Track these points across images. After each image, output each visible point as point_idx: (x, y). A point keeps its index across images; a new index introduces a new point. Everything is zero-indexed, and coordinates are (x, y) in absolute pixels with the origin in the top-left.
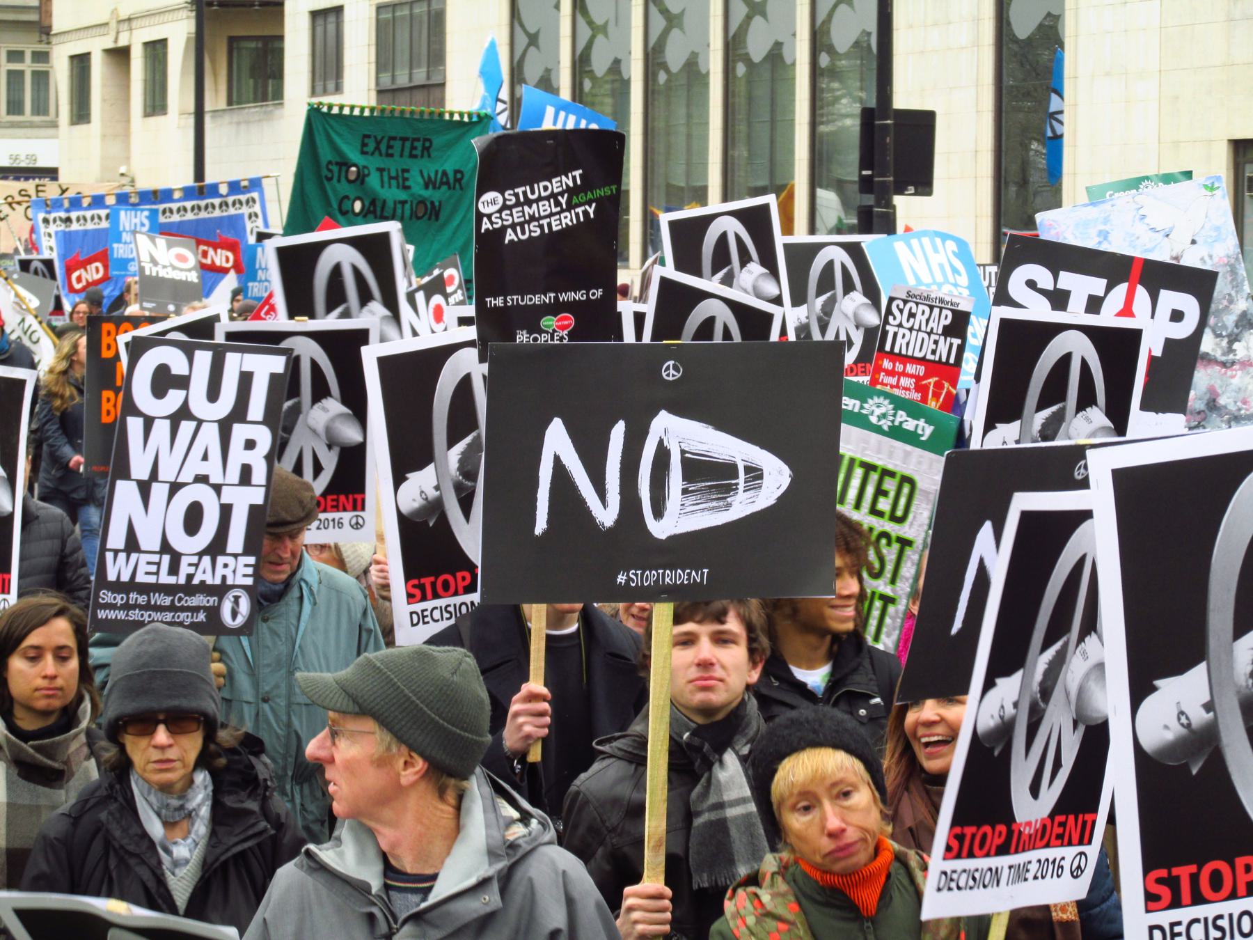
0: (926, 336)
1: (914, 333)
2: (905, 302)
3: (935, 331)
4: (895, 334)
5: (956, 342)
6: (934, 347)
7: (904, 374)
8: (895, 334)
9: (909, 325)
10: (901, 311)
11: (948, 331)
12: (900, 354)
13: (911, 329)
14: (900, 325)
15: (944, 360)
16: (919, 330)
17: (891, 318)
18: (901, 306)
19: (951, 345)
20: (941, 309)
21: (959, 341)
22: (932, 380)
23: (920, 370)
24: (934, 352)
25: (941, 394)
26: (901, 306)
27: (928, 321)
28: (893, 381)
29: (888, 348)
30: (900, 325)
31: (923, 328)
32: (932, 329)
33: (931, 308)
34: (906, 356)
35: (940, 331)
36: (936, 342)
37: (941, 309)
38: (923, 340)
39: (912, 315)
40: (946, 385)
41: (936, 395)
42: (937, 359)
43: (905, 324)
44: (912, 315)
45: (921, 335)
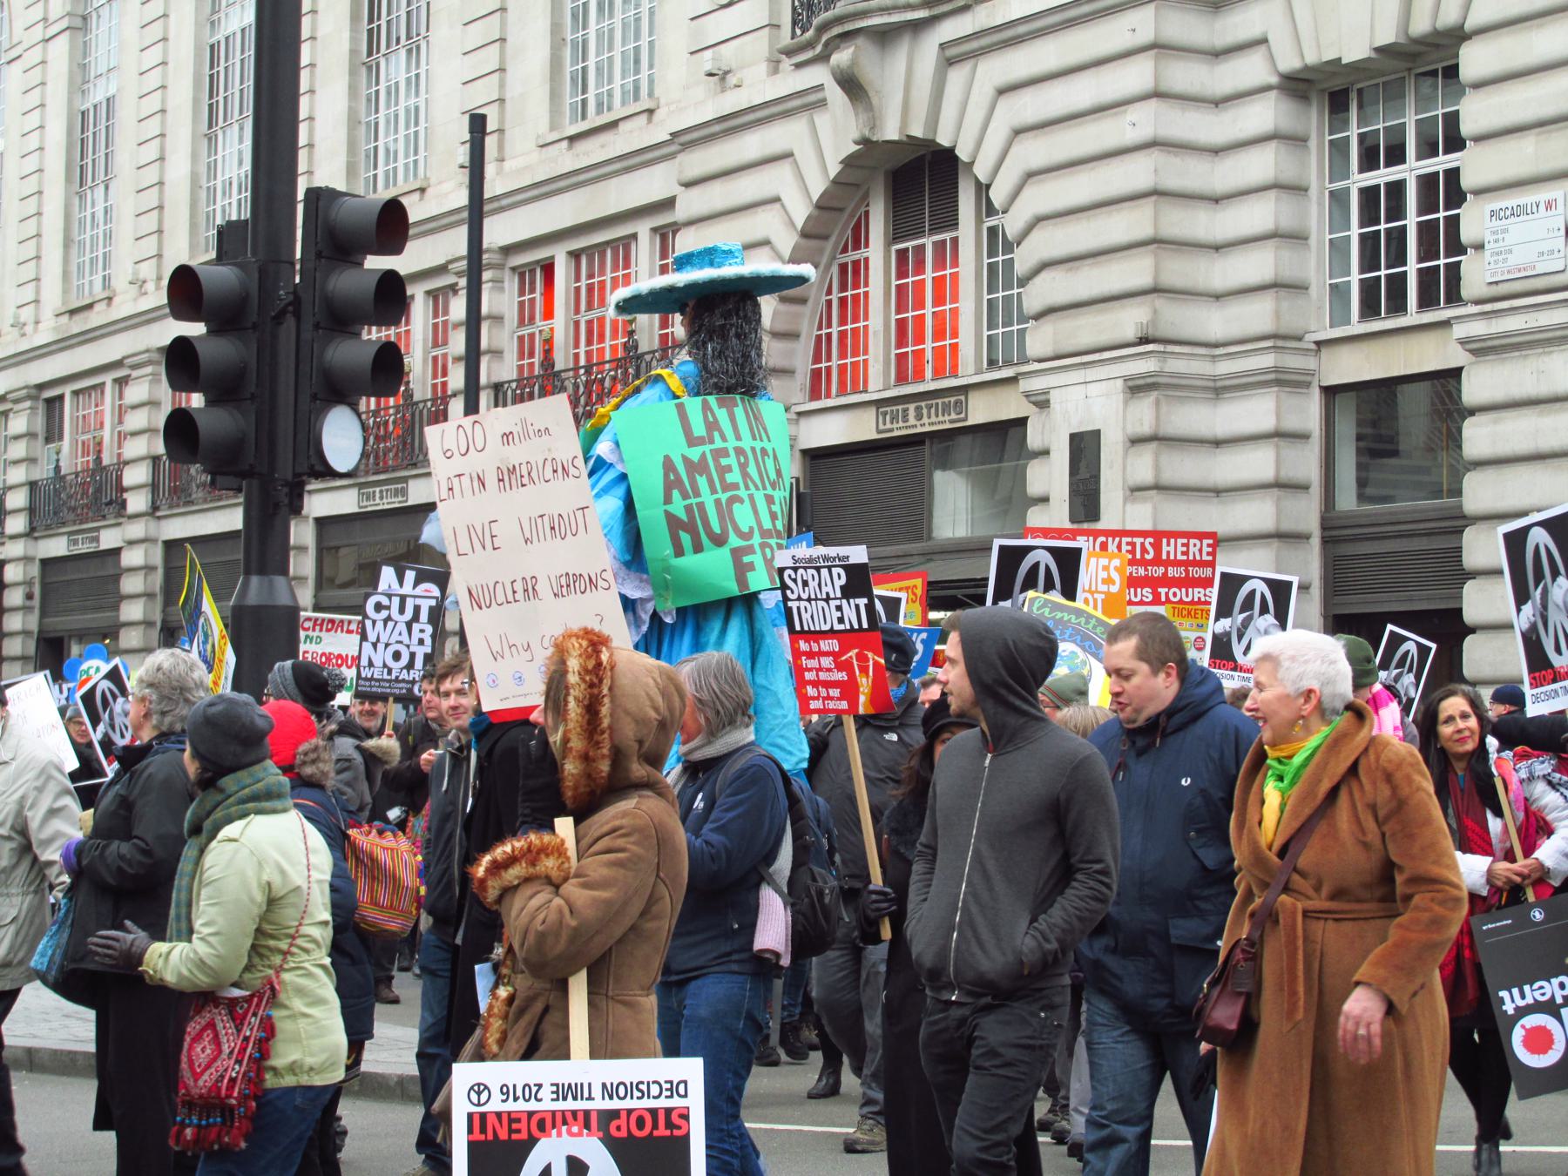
2: (795, 569)
3: (832, 596)
5: (862, 602)
6: (839, 614)
7: (821, 654)
8: (799, 608)
9: (805, 596)
11: (848, 592)
12: (810, 632)
13: (809, 600)
14: (799, 599)
15: (856, 626)
17: (788, 592)
18: (793, 576)
19: (857, 607)
20: (829, 568)
21: (865, 601)
22: (853, 653)
24: (841, 620)
29: (798, 628)
32: (827, 594)
33: (818, 569)
34: (815, 632)
35: (839, 594)
36: (839, 608)
39: (805, 583)
40: (870, 655)
41: (864, 670)
42: (848, 627)
44: (805, 583)
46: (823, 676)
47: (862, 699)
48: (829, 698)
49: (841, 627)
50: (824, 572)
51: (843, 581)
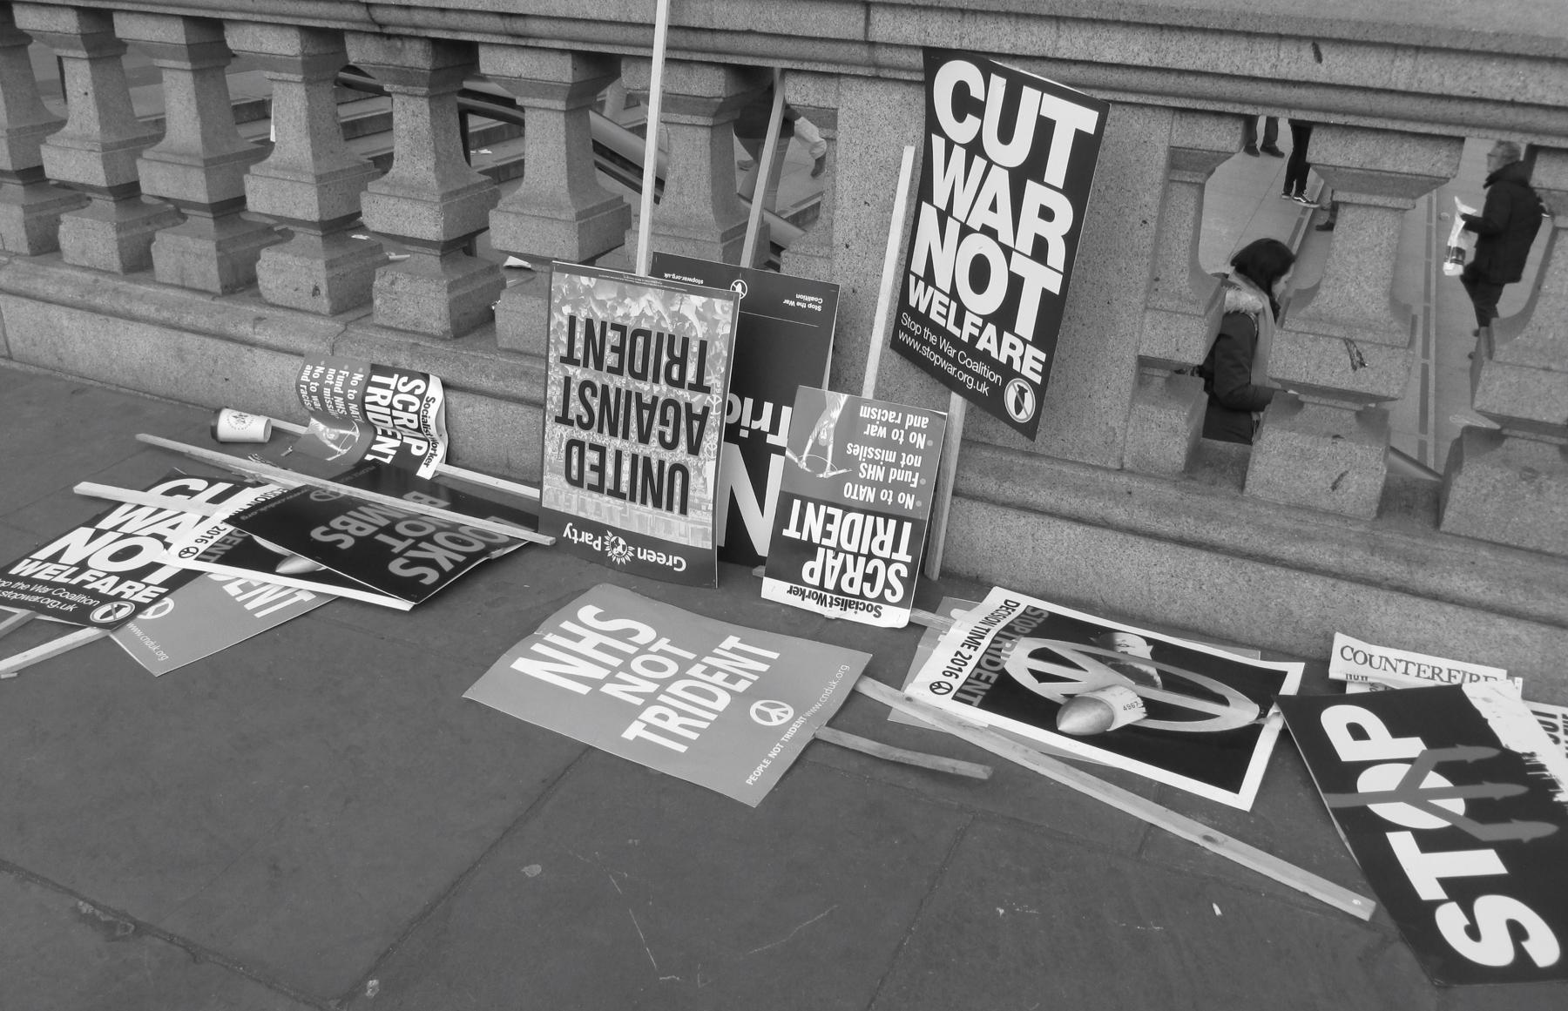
0: (845, 545)
1: (864, 550)
3: (830, 553)
4: (895, 548)
5: (791, 532)
6: (829, 527)
7: (878, 486)
8: (895, 548)
10: (887, 585)
11: (808, 550)
15: (810, 506)
16: (856, 555)
18: (888, 593)
19: (800, 528)
20: (821, 586)
21: (786, 533)
22: (828, 473)
23: (850, 492)
24: (829, 519)
25: (810, 452)
26: (888, 593)
27: (843, 570)
28: (895, 474)
30: (888, 562)
31: (850, 558)
34: (876, 514)
35: (821, 551)
36: (826, 534)
37: (821, 586)
38: (849, 541)
40: (803, 465)
41: (819, 449)
43: (881, 565)
45: (853, 547)
46: (891, 457)
47: (836, 414)
48: (890, 427)
49: (831, 510)
50: (830, 584)
51: (808, 566)
